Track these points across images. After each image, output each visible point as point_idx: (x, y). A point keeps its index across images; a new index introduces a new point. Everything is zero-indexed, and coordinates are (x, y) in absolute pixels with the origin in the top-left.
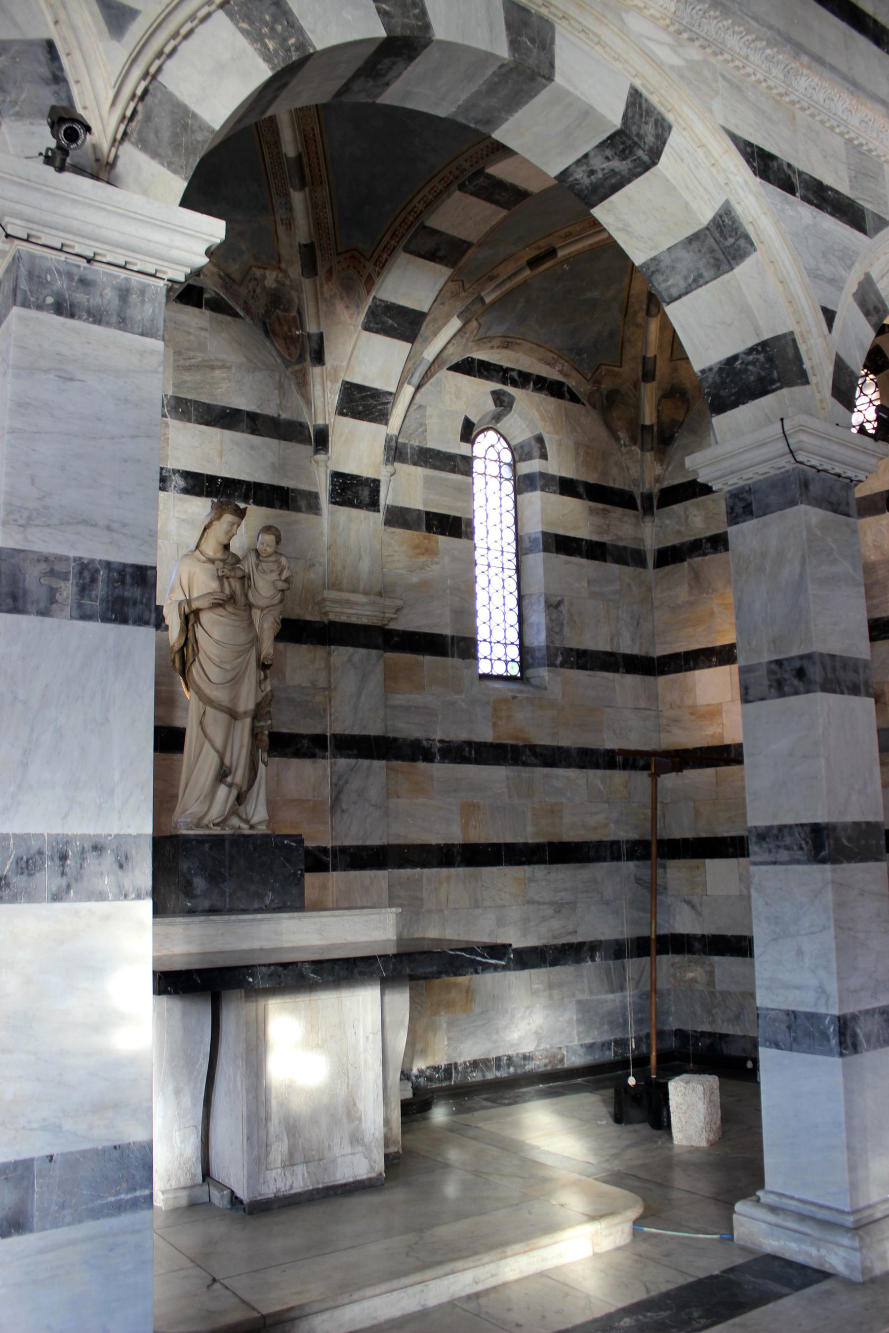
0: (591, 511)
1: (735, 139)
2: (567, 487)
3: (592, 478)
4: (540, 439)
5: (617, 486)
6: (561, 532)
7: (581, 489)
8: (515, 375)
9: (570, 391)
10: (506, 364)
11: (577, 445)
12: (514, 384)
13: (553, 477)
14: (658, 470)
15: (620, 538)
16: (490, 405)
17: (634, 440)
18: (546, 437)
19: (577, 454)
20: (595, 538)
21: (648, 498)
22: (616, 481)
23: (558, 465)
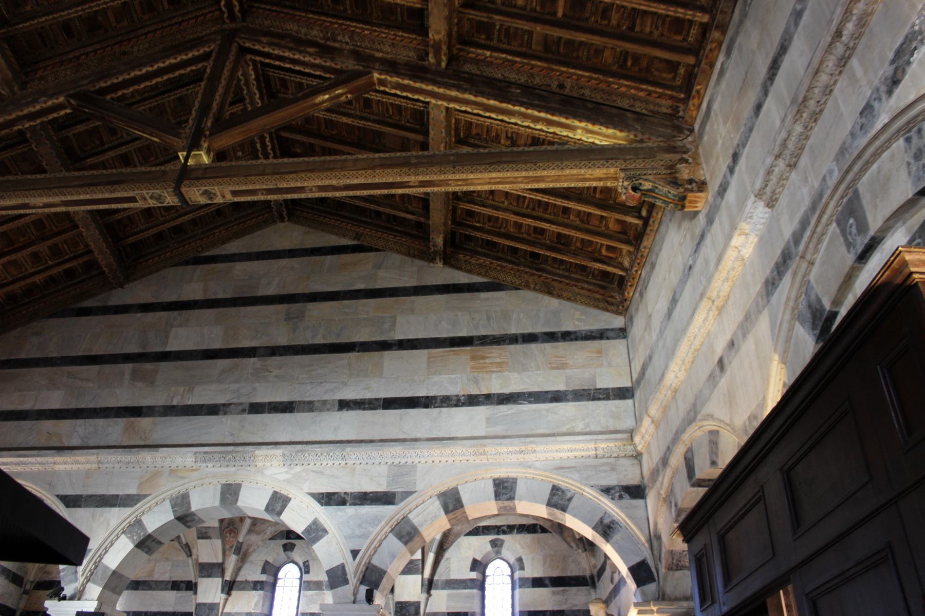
0: (554, 593)
1: (313, 495)
2: (537, 582)
3: (555, 574)
4: (520, 560)
5: (574, 574)
6: (532, 609)
7: (547, 582)
8: (505, 528)
9: (541, 527)
10: (499, 524)
11: (545, 557)
12: (504, 533)
13: (527, 579)
14: (593, 561)
15: (576, 605)
16: (489, 548)
17: (577, 546)
18: (524, 558)
19: (545, 562)
20: (556, 608)
21: (592, 577)
22: (573, 571)
23: (532, 571)
